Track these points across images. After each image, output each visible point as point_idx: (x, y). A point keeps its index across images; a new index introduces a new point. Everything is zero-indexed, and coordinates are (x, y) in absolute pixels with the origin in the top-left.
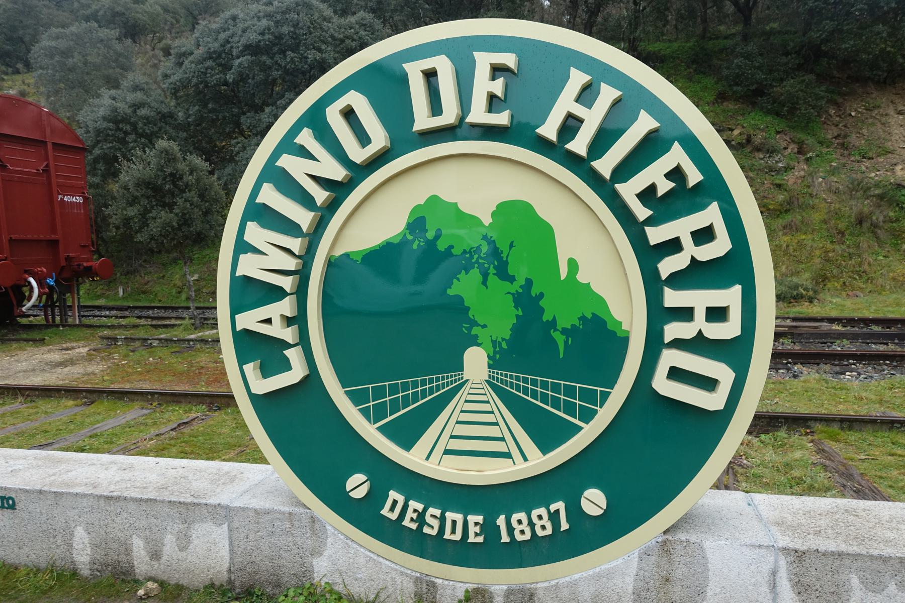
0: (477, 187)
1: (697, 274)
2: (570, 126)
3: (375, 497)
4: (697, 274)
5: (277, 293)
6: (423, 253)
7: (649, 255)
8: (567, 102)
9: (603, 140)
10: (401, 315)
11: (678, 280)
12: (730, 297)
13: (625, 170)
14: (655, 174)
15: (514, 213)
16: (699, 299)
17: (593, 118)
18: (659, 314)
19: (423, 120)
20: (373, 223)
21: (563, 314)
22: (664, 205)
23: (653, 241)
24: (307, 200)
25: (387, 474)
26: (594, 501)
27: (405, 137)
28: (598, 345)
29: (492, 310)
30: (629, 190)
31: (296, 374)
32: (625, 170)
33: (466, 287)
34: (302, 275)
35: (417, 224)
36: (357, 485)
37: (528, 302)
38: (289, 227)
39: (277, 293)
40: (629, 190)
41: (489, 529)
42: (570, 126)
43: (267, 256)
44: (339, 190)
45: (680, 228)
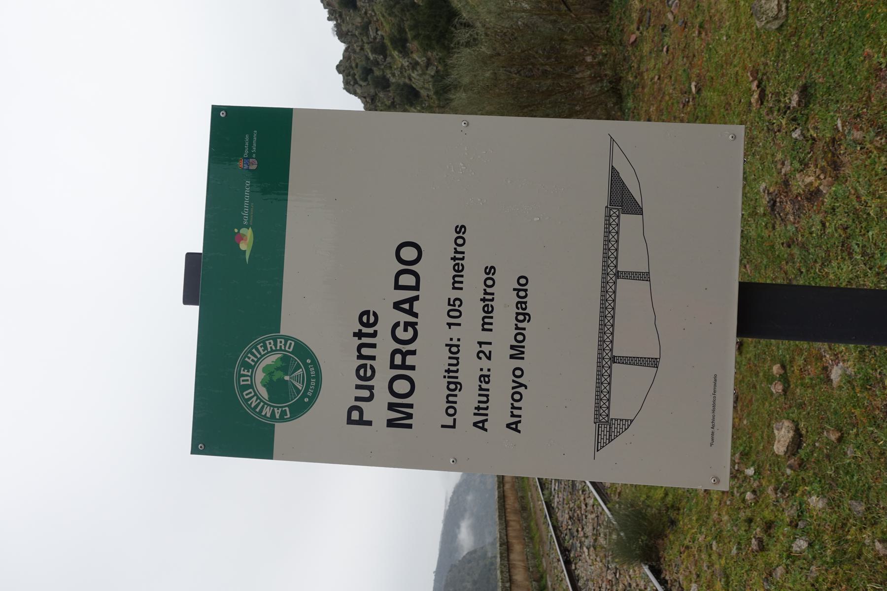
0: (260, 375)
1: (276, 345)
2: (253, 360)
3: (308, 397)
4: (276, 345)
5: (273, 410)
6: (269, 385)
7: (272, 351)
8: (250, 361)
9: (256, 357)
10: (278, 389)
11: (276, 347)
12: (279, 340)
13: (260, 353)
14: (261, 349)
15: (264, 370)
16: (279, 344)
17: (252, 357)
18: (281, 350)
19: (249, 383)
20: (264, 393)
21: (279, 364)
22: (265, 348)
23: (400, 363)
24: (259, 404)
25: (305, 395)
26: (309, 361)
27: (251, 386)
28: (285, 359)
29: (278, 375)
30: (263, 353)
31: (287, 409)
32: (260, 353)
33: (275, 379)
34: (271, 406)
35: (264, 386)
36: (306, 400)
37: (278, 369)
38: (263, 407)
39: (273, 410)
40: (263, 353)
41: (313, 378)
42: (253, 360)
43: (267, 411)
44: (258, 398)
45: (269, 346)
